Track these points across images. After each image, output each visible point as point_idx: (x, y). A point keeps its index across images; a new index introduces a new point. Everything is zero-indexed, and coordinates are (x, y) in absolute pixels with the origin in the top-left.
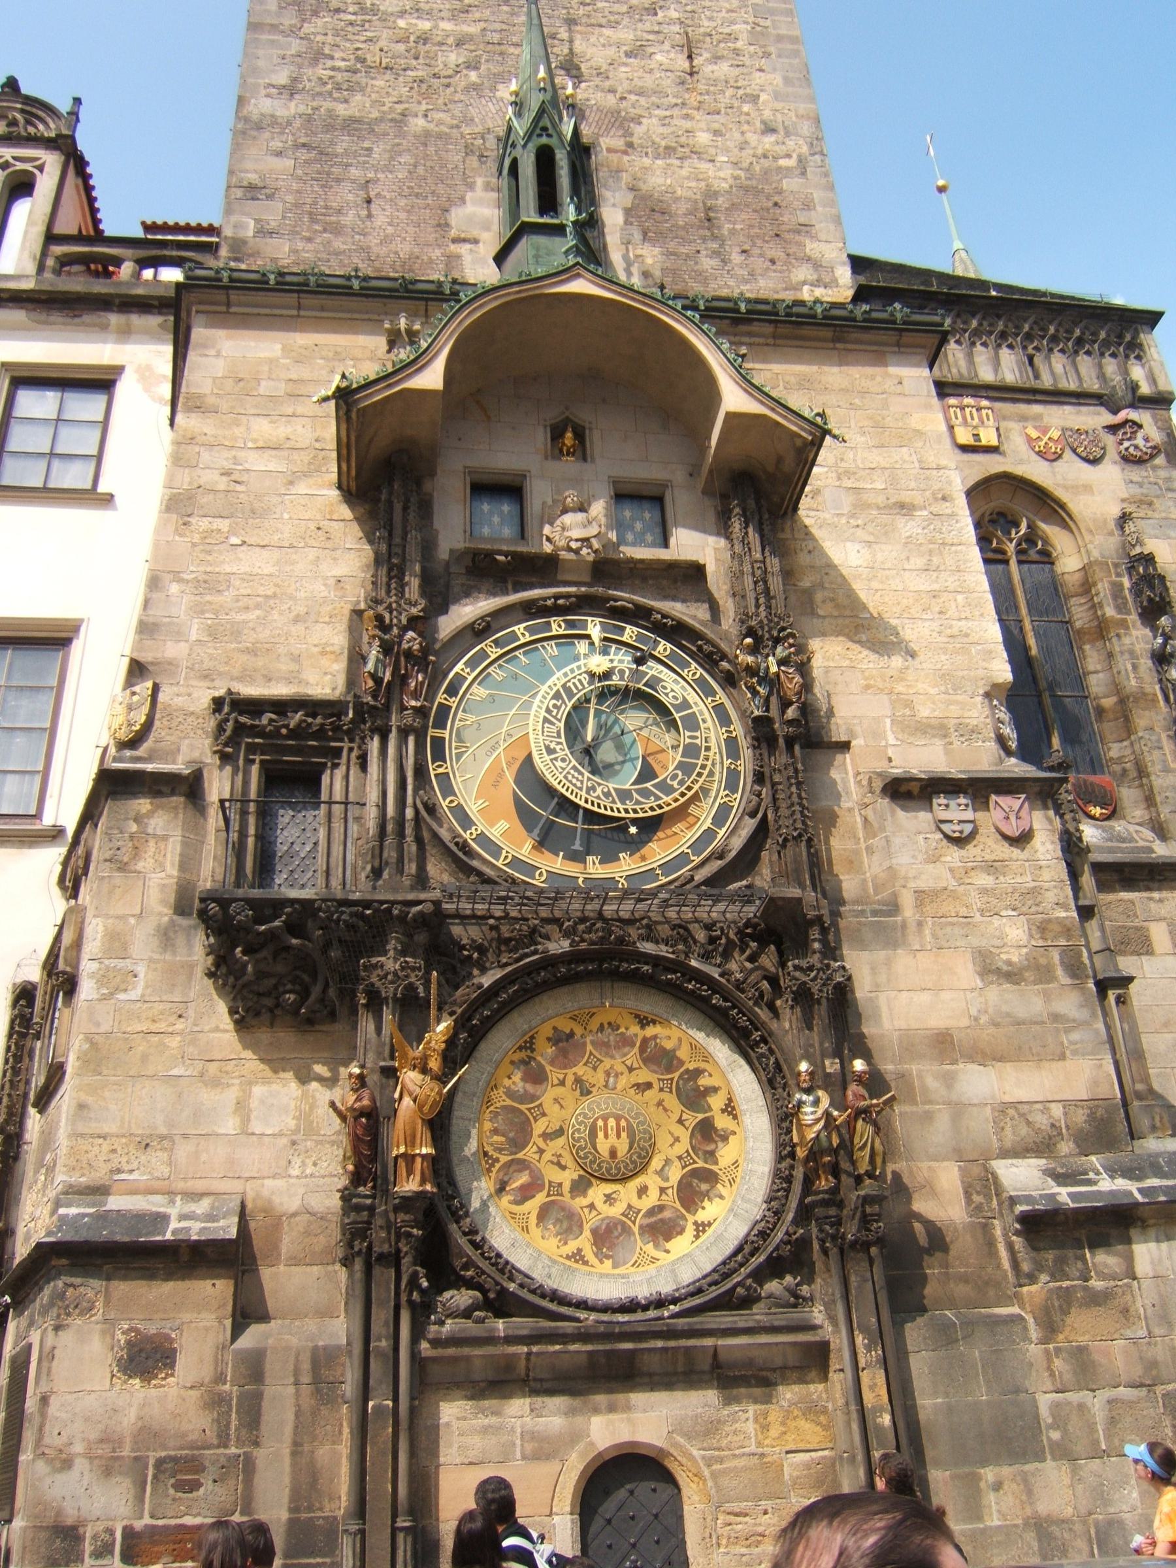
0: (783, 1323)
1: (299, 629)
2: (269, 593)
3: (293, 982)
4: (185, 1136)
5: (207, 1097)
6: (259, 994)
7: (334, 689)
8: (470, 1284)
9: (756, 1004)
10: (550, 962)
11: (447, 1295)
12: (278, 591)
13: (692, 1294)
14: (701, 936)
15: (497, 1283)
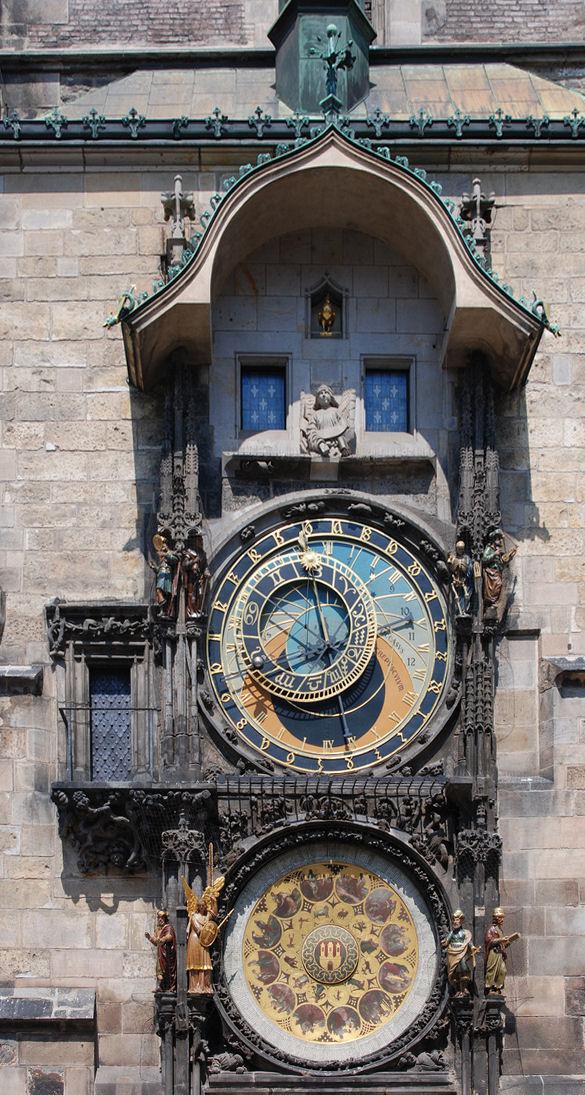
0: (428, 1081)
1: (105, 535)
2: (81, 499)
3: (118, 846)
4: (58, 950)
5: (69, 923)
6: (96, 853)
7: (135, 593)
8: (233, 1051)
9: (433, 864)
10: (291, 832)
11: (222, 1055)
12: (88, 497)
13: (373, 1061)
14: (402, 808)
15: (252, 1051)
